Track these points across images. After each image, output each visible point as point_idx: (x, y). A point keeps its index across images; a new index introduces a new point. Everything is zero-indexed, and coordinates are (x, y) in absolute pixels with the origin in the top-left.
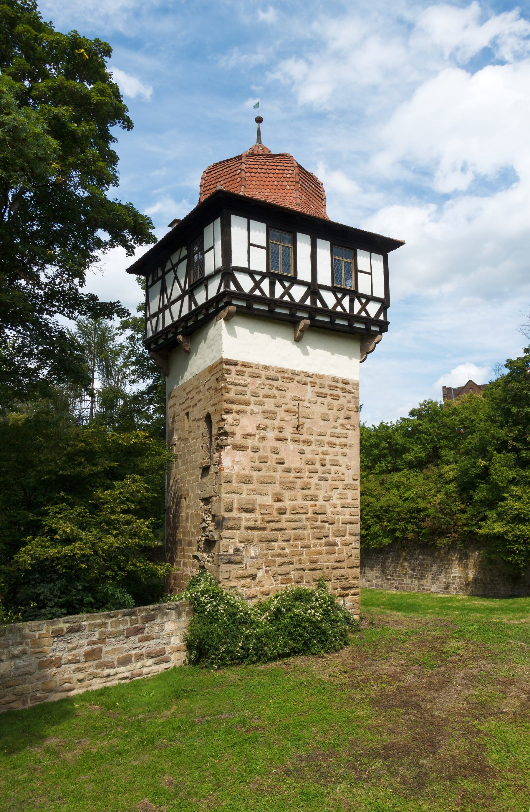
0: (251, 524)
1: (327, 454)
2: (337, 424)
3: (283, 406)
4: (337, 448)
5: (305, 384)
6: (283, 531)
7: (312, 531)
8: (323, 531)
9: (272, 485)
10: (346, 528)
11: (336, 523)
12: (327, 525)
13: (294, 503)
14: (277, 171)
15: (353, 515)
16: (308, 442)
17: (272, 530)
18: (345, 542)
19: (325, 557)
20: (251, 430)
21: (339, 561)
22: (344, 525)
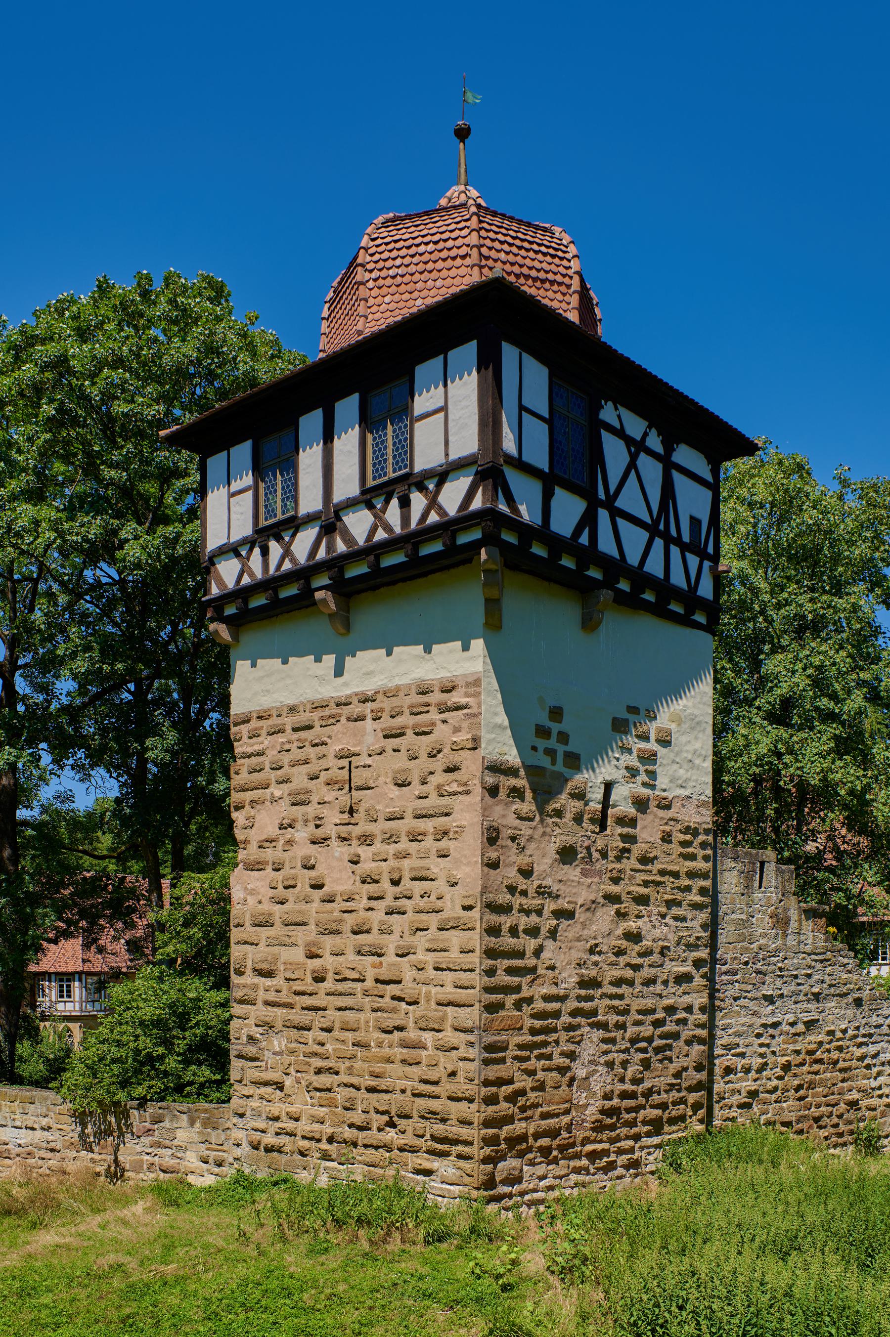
0: (272, 996)
1: (406, 856)
2: (429, 789)
3: (323, 773)
4: (429, 842)
5: (360, 718)
6: (320, 1012)
7: (374, 1014)
8: (395, 1016)
9: (303, 928)
10: (445, 1014)
11: (422, 1001)
12: (403, 1005)
13: (340, 959)
15: (461, 987)
16: (366, 839)
17: (303, 1009)
18: (441, 1042)
19: (396, 1069)
21: (426, 1082)
22: (440, 1008)
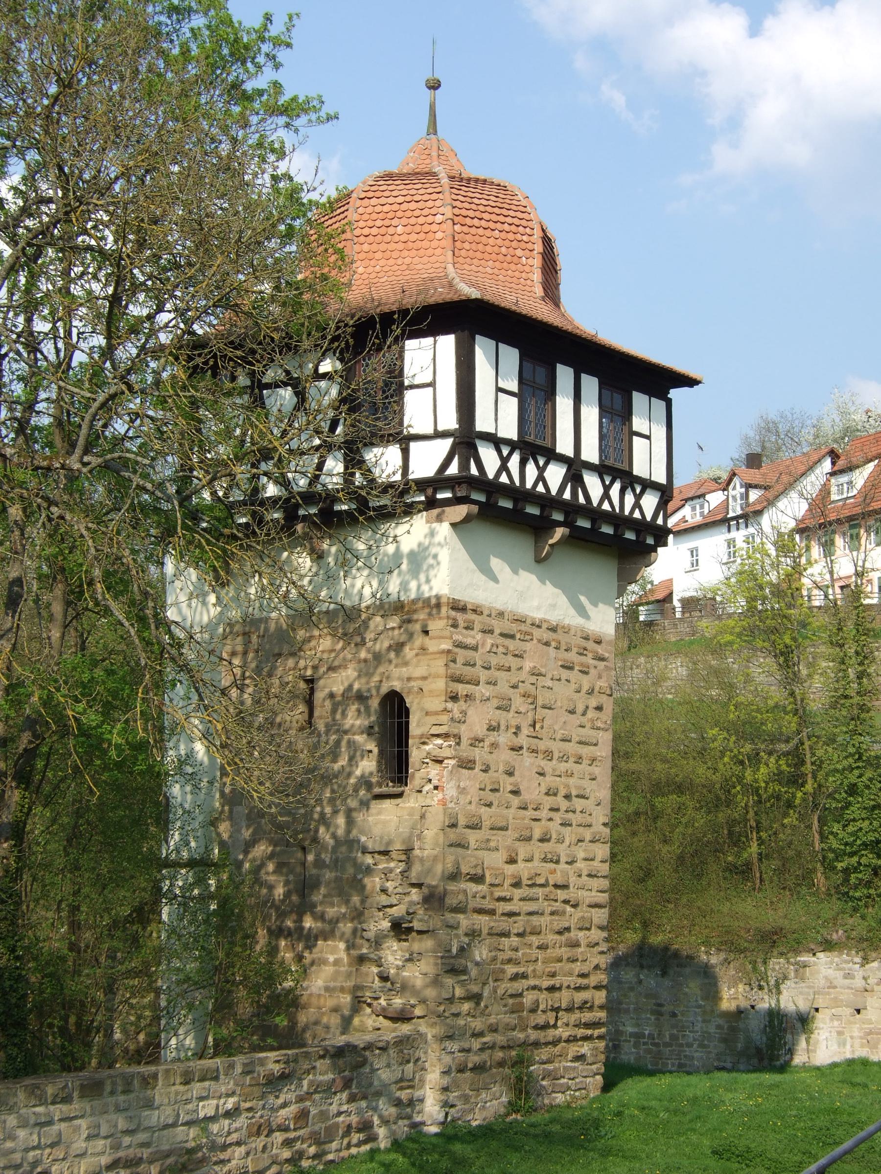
9: (503, 833)
14: (506, 227)
16: (548, 755)
20: (480, 730)
